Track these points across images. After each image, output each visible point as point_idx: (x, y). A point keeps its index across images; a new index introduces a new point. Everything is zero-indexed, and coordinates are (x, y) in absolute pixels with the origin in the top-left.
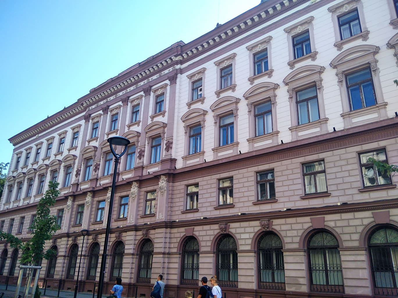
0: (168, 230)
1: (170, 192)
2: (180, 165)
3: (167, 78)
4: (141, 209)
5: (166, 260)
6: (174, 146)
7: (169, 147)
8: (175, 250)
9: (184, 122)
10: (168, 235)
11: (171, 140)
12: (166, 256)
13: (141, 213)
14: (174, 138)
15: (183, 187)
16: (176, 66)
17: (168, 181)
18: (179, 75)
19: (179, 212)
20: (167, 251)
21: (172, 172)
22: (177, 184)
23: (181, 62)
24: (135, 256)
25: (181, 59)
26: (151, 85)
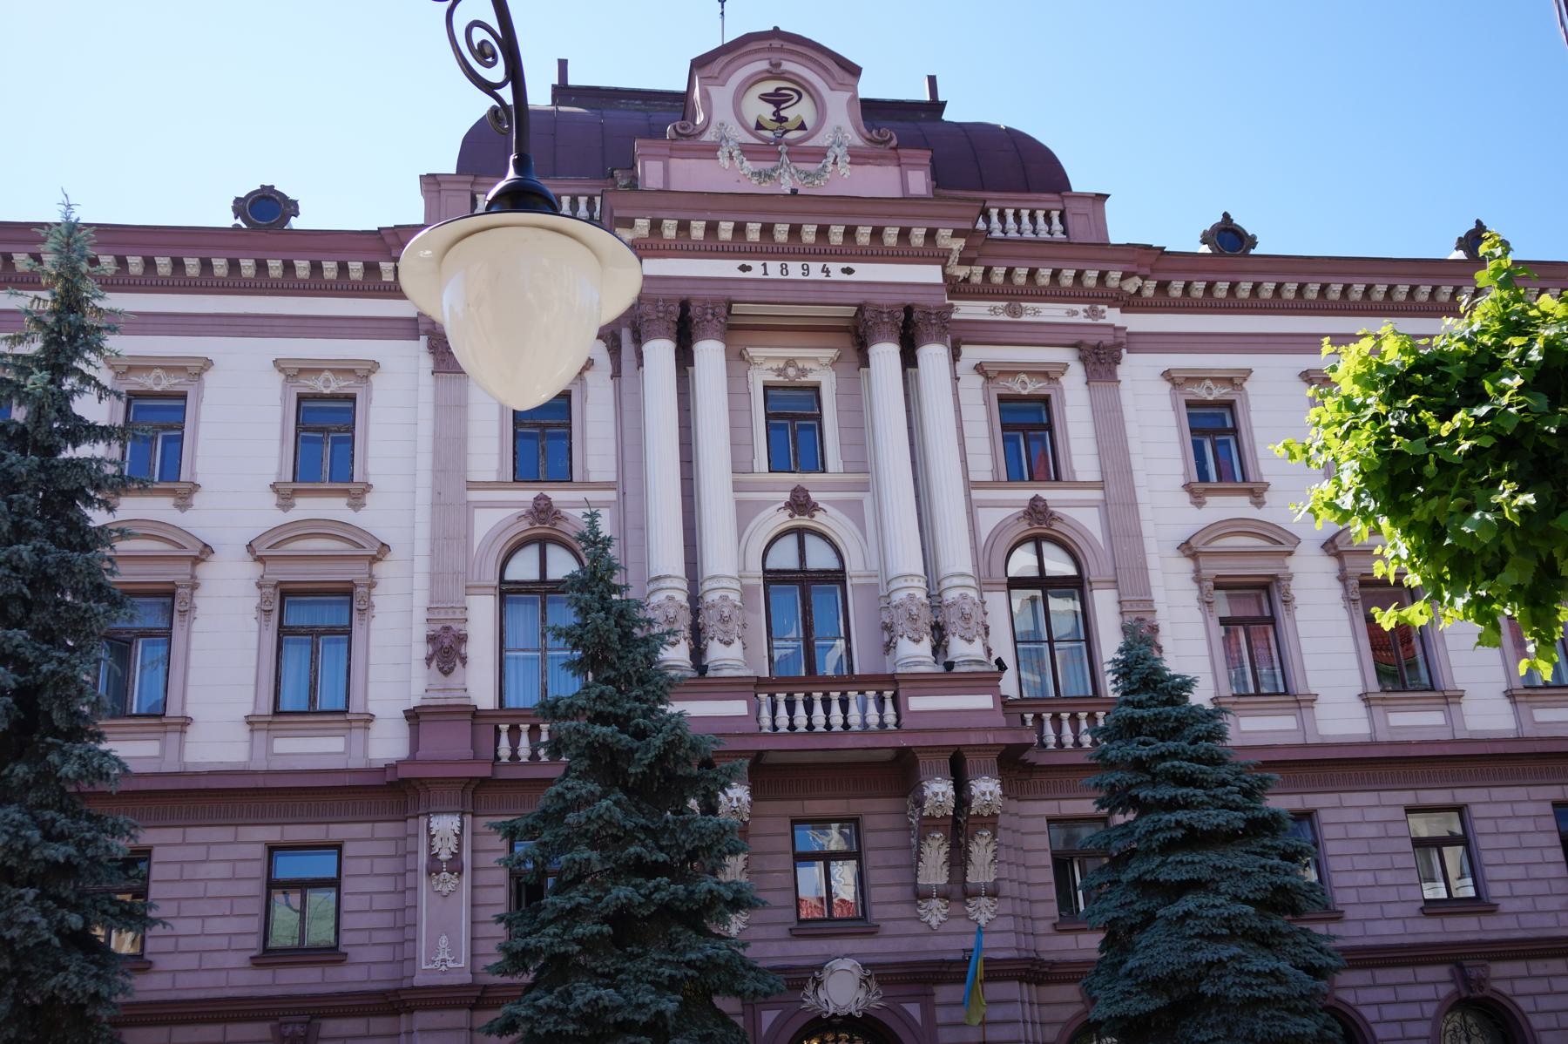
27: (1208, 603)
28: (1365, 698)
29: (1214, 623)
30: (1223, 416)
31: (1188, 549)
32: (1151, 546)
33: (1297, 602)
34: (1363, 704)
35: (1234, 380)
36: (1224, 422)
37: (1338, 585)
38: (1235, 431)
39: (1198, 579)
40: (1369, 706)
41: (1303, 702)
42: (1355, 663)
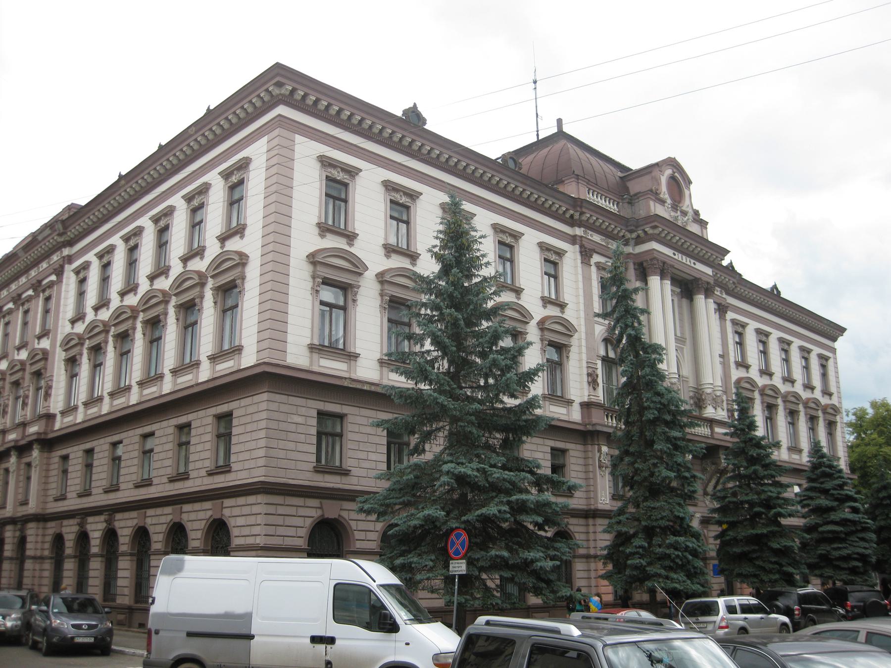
0: (41, 525)
1: (44, 467)
2: (57, 426)
3: (52, 271)
4: (20, 490)
5: (37, 567)
6: (53, 392)
7: (47, 395)
8: (46, 553)
9: (65, 351)
10: (40, 532)
11: (49, 382)
12: (38, 561)
13: (20, 497)
14: (55, 379)
15: (107, 447)
16: (63, 249)
17: (42, 450)
18: (67, 266)
19: (51, 499)
20: (39, 553)
21: (43, 437)
22: (54, 454)
23: (71, 243)
24: (15, 561)
25: (67, 239)
26: (40, 278)
27: (317, 291)
28: (381, 362)
29: (317, 303)
30: (340, 190)
31: (313, 259)
32: (293, 252)
33: (358, 303)
34: (378, 365)
35: (353, 172)
36: (340, 194)
37: (379, 298)
38: (346, 201)
39: (314, 277)
40: (381, 366)
41: (352, 357)
42: (379, 340)
